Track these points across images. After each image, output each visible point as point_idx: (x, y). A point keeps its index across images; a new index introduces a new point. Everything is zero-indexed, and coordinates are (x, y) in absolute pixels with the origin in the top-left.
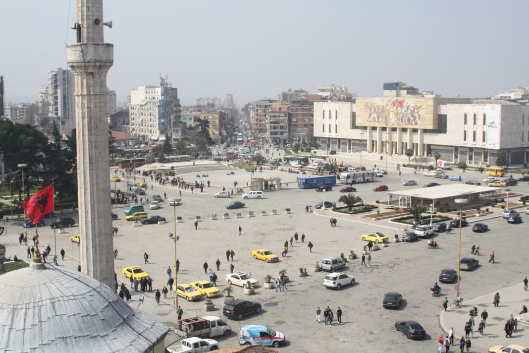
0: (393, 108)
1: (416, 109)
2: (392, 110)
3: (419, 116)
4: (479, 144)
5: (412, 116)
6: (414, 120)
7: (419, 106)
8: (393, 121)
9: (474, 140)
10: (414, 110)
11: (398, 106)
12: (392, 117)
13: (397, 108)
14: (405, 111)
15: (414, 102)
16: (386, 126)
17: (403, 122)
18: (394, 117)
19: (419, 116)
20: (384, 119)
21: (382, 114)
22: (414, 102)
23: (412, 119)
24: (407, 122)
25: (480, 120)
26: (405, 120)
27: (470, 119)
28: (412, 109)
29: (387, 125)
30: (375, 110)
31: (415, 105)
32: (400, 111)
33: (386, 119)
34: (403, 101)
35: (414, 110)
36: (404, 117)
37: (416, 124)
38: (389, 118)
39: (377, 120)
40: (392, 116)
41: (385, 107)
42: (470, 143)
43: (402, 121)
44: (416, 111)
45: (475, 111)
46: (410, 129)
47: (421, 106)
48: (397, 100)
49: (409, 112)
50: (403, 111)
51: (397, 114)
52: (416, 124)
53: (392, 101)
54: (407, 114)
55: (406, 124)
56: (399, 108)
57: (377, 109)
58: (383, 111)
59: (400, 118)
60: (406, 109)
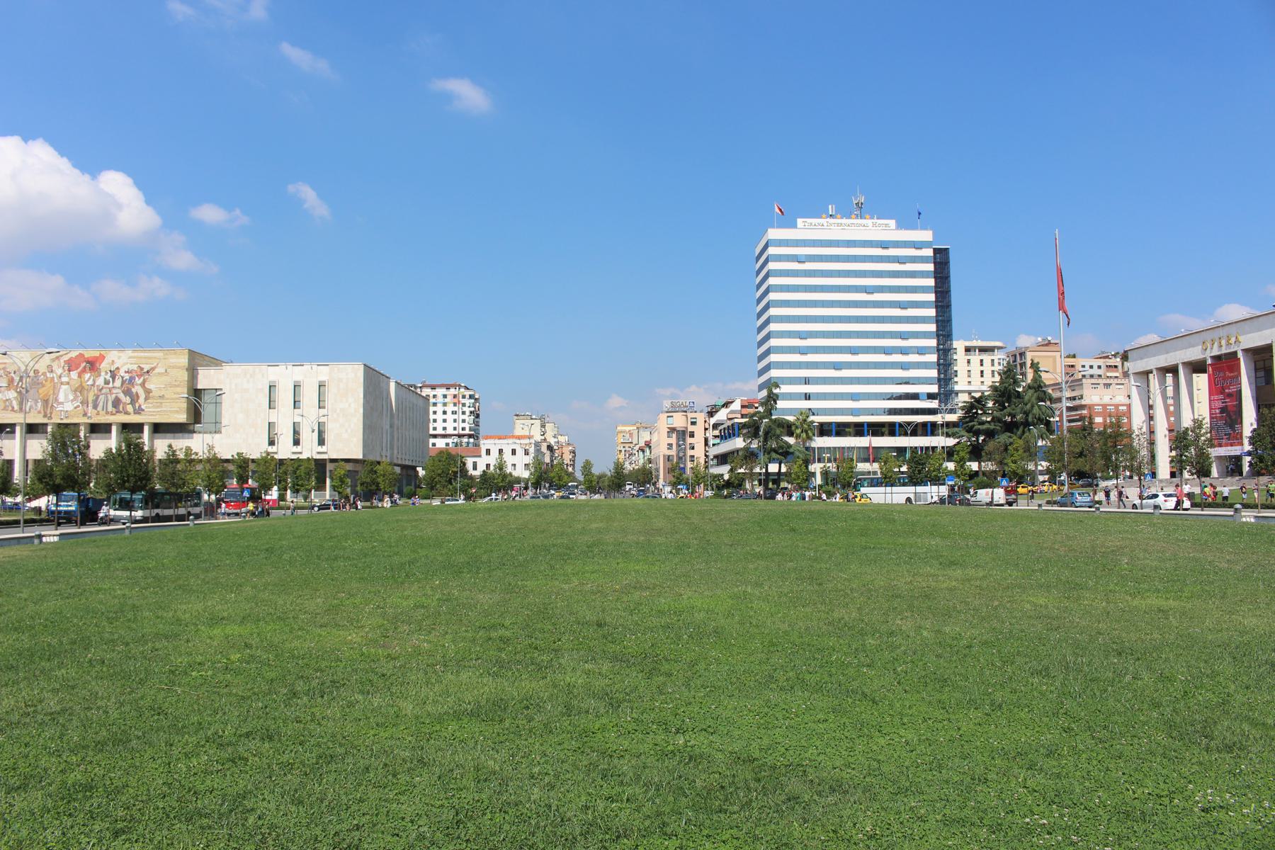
0: (69, 376)
1: (139, 376)
2: (65, 379)
3: (148, 392)
4: (309, 450)
5: (127, 392)
6: (133, 402)
7: (146, 368)
8: (69, 407)
9: (297, 442)
10: (132, 379)
11: (84, 371)
12: (66, 396)
13: (80, 376)
14: (107, 382)
15: (133, 360)
16: (45, 421)
17: (100, 408)
18: (71, 397)
19: (148, 392)
20: (39, 405)
21: (32, 392)
22: (133, 360)
23: (128, 400)
24: (110, 408)
25: (309, 396)
26: (106, 401)
27: (285, 397)
28: (127, 377)
29: (50, 418)
30: (11, 381)
31: (135, 367)
32: (90, 382)
33: (46, 402)
34: (102, 358)
35: (132, 379)
36: (102, 398)
37: (139, 411)
38: (56, 400)
39: (16, 407)
40: (64, 394)
41: (44, 374)
42: (285, 450)
43: (95, 407)
44: (139, 381)
45: (298, 378)
46: (117, 424)
47: (153, 369)
48: (81, 355)
49: (118, 383)
50: (100, 382)
51: (80, 389)
52: (139, 411)
53: (66, 358)
54: (110, 389)
55: (107, 413)
56: (87, 376)
57: (17, 379)
58: (37, 384)
59: (91, 398)
60: (108, 377)
